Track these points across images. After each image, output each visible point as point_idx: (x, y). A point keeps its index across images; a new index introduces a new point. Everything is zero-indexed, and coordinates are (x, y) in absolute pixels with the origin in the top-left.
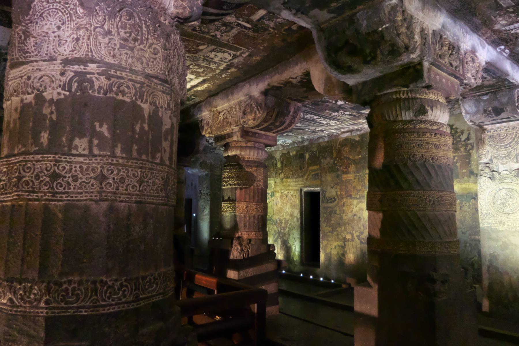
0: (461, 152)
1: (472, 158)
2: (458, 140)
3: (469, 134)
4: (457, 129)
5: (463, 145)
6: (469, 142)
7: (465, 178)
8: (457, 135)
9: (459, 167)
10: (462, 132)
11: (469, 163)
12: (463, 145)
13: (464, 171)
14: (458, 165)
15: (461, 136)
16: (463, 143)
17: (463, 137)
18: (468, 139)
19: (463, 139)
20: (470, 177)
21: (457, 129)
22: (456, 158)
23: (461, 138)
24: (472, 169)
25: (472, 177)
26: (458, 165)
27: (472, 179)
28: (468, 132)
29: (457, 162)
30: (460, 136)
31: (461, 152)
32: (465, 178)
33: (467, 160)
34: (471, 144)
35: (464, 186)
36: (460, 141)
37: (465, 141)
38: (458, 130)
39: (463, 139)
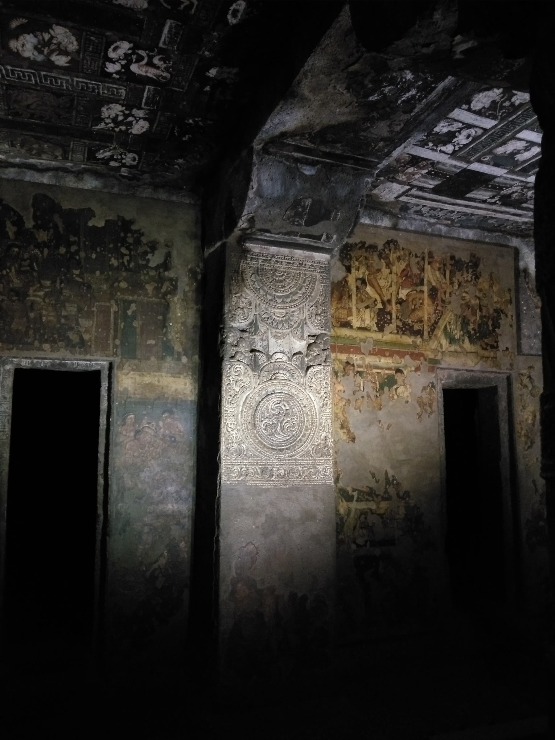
0: (146, 295)
1: (170, 315)
2: (141, 262)
3: (168, 255)
4: (142, 234)
5: (152, 279)
6: (166, 273)
7: (153, 359)
8: (140, 250)
9: (138, 330)
10: (153, 247)
11: (164, 324)
12: (152, 279)
13: (151, 342)
14: (135, 324)
15: (149, 256)
16: (152, 273)
17: (155, 260)
18: (166, 265)
19: (152, 264)
20: (163, 358)
21: (142, 234)
22: (133, 307)
23: (148, 261)
24: (169, 341)
25: (169, 359)
26: (135, 324)
27: (167, 365)
28: (165, 251)
29: (134, 317)
30: (146, 253)
31: (146, 295)
32: (153, 359)
33: (160, 318)
34: (171, 280)
35: (147, 379)
36: (146, 266)
37: (157, 268)
38: (144, 240)
39: (152, 264)
